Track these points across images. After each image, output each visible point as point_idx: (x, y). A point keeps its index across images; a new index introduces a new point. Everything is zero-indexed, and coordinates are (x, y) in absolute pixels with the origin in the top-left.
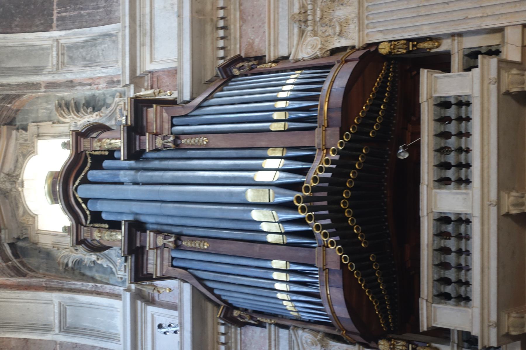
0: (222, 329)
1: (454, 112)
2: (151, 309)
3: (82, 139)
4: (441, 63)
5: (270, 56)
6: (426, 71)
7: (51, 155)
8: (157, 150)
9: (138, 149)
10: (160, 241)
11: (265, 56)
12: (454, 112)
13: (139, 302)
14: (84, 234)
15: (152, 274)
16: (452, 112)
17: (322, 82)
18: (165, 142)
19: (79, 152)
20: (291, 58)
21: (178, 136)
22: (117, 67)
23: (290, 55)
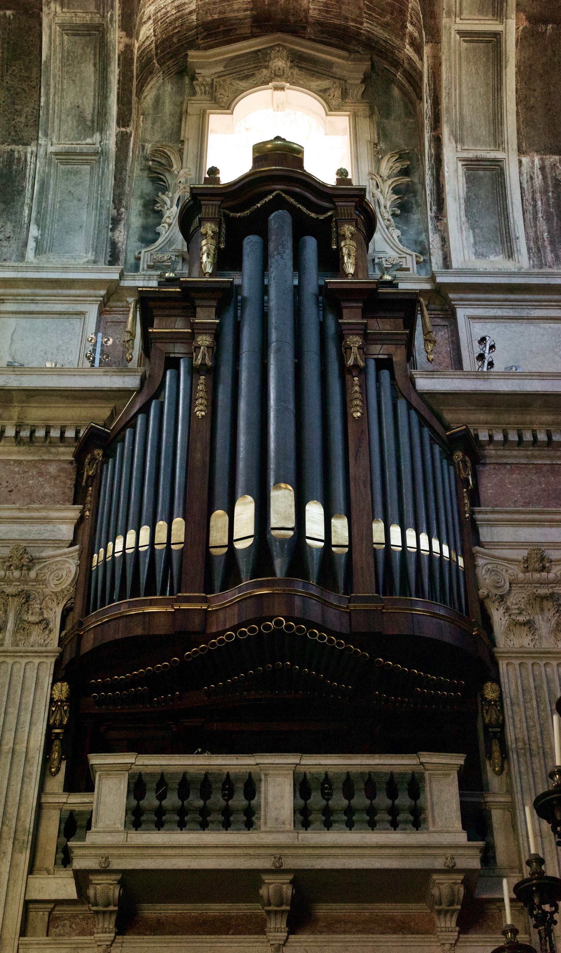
0: (70, 434)
1: (402, 803)
2: (93, 311)
3: (354, 204)
4: (471, 782)
5: (480, 512)
6: (462, 762)
7: (329, 146)
8: (340, 337)
9: (344, 304)
10: (204, 340)
11: (480, 506)
12: (402, 803)
13: (103, 292)
14: (210, 208)
15: (152, 327)
16: (403, 800)
17: (444, 601)
18: (355, 350)
19: (335, 200)
20: (478, 548)
21: (363, 372)
22: (465, 253)
23: (482, 547)
